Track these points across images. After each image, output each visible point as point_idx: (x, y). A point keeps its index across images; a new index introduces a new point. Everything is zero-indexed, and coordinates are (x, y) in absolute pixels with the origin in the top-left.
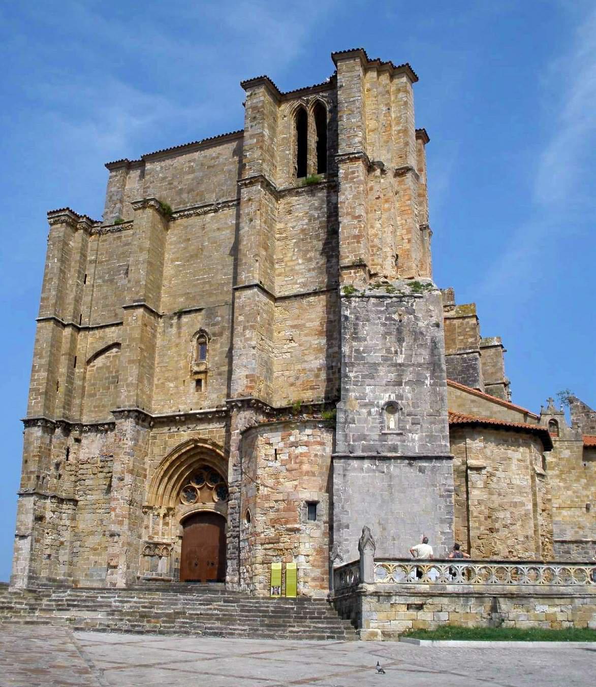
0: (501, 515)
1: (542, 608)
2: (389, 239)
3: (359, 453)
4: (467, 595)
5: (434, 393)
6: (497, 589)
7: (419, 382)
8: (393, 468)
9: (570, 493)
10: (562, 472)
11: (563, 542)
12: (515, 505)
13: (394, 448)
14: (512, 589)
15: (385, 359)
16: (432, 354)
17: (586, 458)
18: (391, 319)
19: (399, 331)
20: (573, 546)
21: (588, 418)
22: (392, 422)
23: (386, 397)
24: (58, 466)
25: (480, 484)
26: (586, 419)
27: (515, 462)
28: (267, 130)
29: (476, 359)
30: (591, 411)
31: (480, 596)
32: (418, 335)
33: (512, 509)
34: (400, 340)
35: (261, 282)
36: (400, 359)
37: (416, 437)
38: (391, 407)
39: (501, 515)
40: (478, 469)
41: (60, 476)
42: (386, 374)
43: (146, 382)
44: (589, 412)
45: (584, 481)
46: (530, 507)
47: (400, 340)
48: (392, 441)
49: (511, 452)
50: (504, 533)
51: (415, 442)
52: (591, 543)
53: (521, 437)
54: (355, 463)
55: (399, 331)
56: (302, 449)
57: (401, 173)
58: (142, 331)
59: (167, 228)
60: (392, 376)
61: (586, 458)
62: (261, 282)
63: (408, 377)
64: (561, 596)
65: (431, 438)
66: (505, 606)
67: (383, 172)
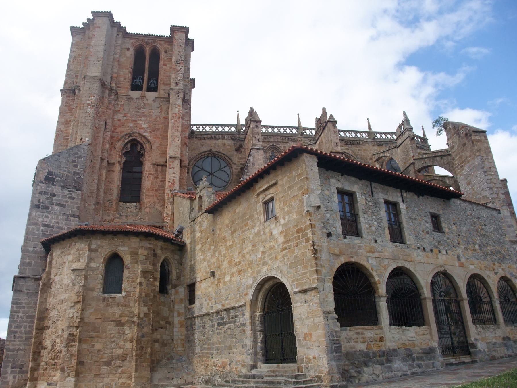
9: (206, 263)
21: (459, 137)
26: (458, 139)
27: (67, 263)
30: (460, 128)
33: (59, 307)
44: (458, 130)
45: (212, 248)
52: (215, 314)
53: (73, 241)
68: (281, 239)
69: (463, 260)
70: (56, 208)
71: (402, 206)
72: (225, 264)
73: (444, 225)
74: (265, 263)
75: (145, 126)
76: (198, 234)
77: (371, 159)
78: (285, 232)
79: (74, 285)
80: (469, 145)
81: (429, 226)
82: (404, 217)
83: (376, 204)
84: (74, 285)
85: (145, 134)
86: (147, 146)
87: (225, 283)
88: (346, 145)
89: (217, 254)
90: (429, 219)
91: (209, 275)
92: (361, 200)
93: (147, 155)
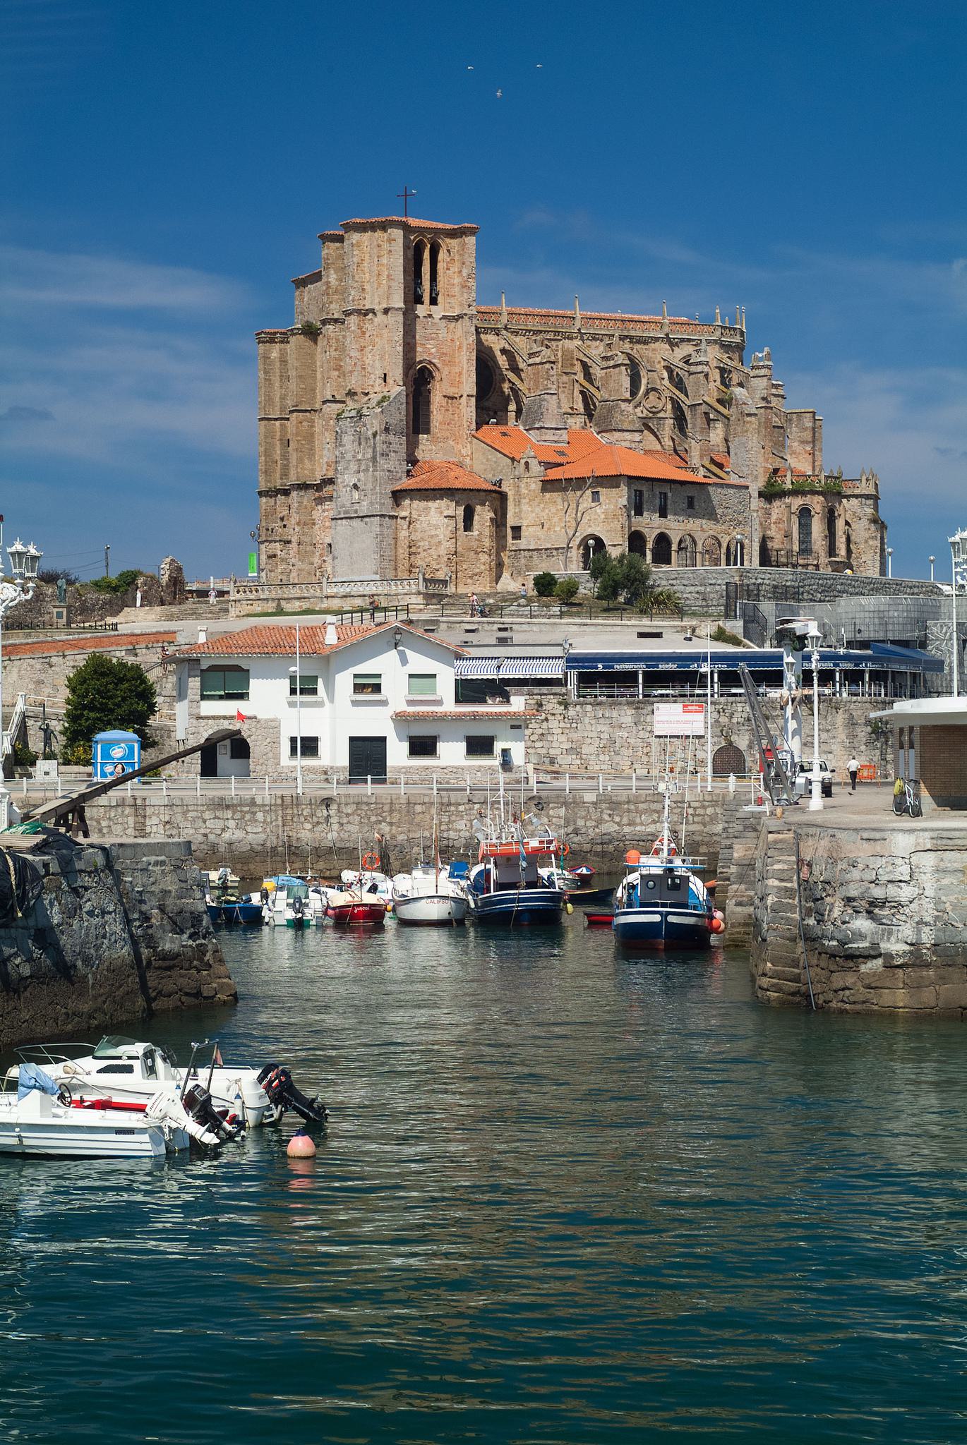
0: (421, 544)
1: (297, 603)
2: (378, 364)
3: (342, 516)
4: (267, 600)
5: (374, 476)
6: (278, 597)
7: (367, 470)
8: (356, 523)
10: (530, 500)
11: (529, 550)
12: (432, 536)
13: (356, 511)
14: (285, 596)
15: (354, 457)
16: (374, 452)
17: (544, 490)
18: (355, 431)
19: (360, 439)
20: (535, 553)
22: (356, 495)
23: (354, 481)
24: (282, 519)
25: (405, 527)
28: (335, 276)
29: (545, 400)
31: (273, 599)
32: (368, 439)
34: (360, 444)
35: (333, 396)
36: (360, 457)
37: (365, 503)
38: (355, 487)
39: (420, 544)
40: (404, 518)
41: (285, 526)
42: (354, 467)
43: (306, 461)
46: (442, 537)
47: (360, 444)
48: (356, 507)
49: (430, 504)
50: (423, 554)
51: (364, 509)
54: (339, 521)
55: (360, 439)
56: (326, 513)
57: (386, 311)
58: (297, 428)
59: (315, 342)
60: (356, 467)
61: (544, 490)
62: (333, 396)
63: (363, 467)
64: (304, 598)
65: (372, 504)
66: (283, 603)
67: (375, 313)
68: (603, 516)
69: (704, 526)
70: (393, 454)
71: (670, 495)
72: (556, 519)
73: (696, 503)
74: (590, 526)
75: (433, 350)
76: (524, 491)
77: (659, 362)
78: (606, 513)
79: (448, 526)
80: (741, 422)
81: (685, 505)
82: (669, 502)
83: (654, 496)
84: (448, 526)
85: (434, 361)
86: (436, 374)
87: (555, 531)
88: (630, 342)
89: (547, 511)
90: (686, 501)
91: (539, 523)
92: (646, 495)
93: (437, 385)
